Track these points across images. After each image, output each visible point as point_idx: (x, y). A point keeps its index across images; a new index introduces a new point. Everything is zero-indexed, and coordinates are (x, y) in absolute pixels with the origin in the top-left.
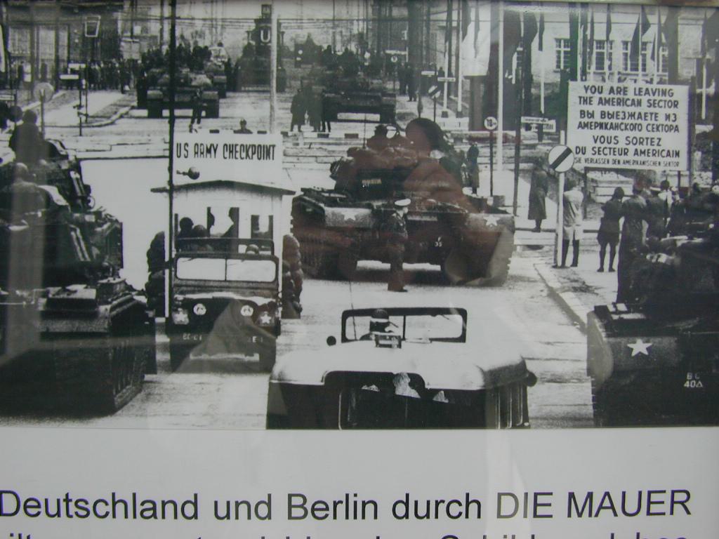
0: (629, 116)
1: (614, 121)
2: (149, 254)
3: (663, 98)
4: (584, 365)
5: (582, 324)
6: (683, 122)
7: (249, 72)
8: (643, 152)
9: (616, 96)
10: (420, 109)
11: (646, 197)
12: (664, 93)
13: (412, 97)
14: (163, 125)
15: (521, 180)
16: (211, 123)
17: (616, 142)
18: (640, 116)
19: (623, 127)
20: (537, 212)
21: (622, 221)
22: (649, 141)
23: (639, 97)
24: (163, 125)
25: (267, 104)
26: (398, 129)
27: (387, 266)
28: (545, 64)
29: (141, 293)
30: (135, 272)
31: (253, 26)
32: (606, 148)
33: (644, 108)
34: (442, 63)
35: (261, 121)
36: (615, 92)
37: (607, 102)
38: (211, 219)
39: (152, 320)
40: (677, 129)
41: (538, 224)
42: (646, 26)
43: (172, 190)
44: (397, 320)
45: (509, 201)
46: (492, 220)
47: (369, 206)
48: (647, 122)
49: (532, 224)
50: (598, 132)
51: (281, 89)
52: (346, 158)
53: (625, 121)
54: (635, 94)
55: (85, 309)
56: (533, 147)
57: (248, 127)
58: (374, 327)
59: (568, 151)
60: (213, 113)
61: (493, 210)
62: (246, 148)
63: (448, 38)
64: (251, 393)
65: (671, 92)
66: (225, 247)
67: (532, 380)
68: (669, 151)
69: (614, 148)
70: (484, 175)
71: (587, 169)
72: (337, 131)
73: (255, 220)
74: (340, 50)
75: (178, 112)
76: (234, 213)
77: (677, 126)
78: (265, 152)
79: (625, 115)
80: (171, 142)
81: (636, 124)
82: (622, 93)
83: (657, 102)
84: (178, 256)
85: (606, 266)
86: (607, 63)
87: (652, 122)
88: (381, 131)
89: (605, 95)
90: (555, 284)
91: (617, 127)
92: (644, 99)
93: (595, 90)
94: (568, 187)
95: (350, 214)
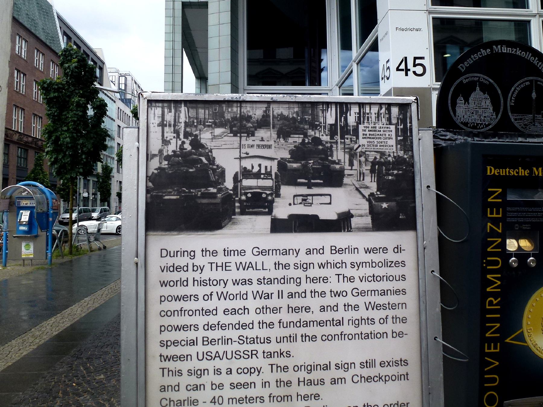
1: (373, 136)
2: (233, 178)
4: (368, 211)
5: (367, 199)
6: (394, 136)
7: (264, 123)
10: (315, 134)
11: (384, 159)
12: (388, 128)
13: (313, 130)
14: (238, 139)
15: (346, 155)
16: (253, 138)
20: (351, 164)
21: (377, 166)
24: (238, 139)
25: (269, 132)
26: (309, 140)
27: (307, 181)
28: (352, 120)
29: (231, 190)
30: (229, 184)
31: (265, 109)
33: (382, 133)
34: (322, 120)
35: (268, 137)
37: (371, 131)
38: (253, 167)
39: (234, 199)
41: (352, 168)
42: (381, 108)
43: (241, 158)
44: (310, 198)
45: (343, 161)
46: (337, 167)
47: (301, 163)
49: (350, 168)
50: (369, 140)
51: (273, 128)
52: (293, 148)
55: (213, 196)
56: (349, 144)
57: (264, 139)
58: (303, 200)
59: (360, 146)
60: (253, 135)
61: (338, 164)
62: (263, 146)
63: (323, 113)
64: (265, 221)
66: (257, 176)
67: (352, 216)
70: (335, 153)
71: (366, 151)
72: (291, 140)
73: (266, 167)
74: (291, 116)
75: (242, 135)
76: (260, 165)
78: (270, 147)
80: (240, 144)
84: (243, 179)
85: (373, 180)
86: (370, 119)
88: (303, 140)
89: (370, 129)
90: (358, 186)
91: (374, 138)
93: (367, 127)
94: (360, 156)
95: (295, 165)
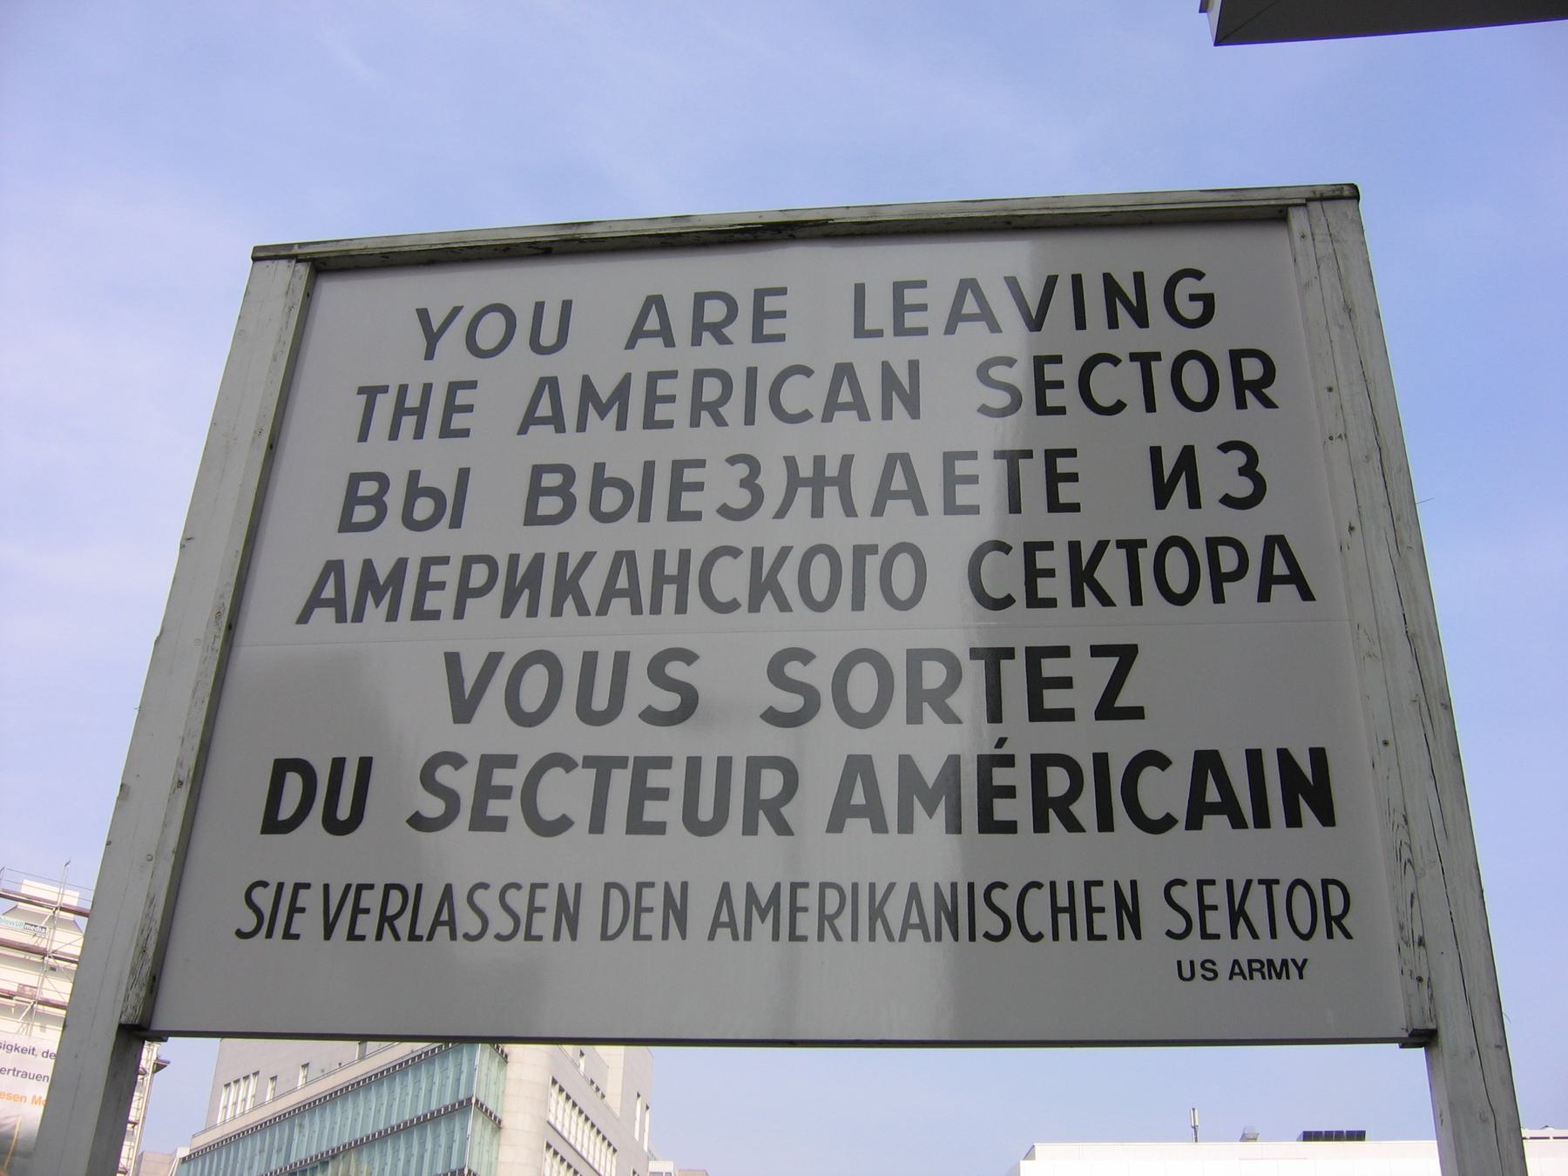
0: (794, 481)
1: (648, 537)
3: (1128, 337)
9: (686, 358)
17: (669, 701)
19: (731, 579)
22: (1014, 674)
23: (899, 351)
32: (561, 761)
40: (1281, 569)
50: (486, 631)
54: (860, 331)
65: (1186, 287)
68: (1207, 763)
69: (644, 765)
77: (1275, 543)
79: (749, 483)
82: (740, 329)
83: (1067, 372)
91: (679, 581)
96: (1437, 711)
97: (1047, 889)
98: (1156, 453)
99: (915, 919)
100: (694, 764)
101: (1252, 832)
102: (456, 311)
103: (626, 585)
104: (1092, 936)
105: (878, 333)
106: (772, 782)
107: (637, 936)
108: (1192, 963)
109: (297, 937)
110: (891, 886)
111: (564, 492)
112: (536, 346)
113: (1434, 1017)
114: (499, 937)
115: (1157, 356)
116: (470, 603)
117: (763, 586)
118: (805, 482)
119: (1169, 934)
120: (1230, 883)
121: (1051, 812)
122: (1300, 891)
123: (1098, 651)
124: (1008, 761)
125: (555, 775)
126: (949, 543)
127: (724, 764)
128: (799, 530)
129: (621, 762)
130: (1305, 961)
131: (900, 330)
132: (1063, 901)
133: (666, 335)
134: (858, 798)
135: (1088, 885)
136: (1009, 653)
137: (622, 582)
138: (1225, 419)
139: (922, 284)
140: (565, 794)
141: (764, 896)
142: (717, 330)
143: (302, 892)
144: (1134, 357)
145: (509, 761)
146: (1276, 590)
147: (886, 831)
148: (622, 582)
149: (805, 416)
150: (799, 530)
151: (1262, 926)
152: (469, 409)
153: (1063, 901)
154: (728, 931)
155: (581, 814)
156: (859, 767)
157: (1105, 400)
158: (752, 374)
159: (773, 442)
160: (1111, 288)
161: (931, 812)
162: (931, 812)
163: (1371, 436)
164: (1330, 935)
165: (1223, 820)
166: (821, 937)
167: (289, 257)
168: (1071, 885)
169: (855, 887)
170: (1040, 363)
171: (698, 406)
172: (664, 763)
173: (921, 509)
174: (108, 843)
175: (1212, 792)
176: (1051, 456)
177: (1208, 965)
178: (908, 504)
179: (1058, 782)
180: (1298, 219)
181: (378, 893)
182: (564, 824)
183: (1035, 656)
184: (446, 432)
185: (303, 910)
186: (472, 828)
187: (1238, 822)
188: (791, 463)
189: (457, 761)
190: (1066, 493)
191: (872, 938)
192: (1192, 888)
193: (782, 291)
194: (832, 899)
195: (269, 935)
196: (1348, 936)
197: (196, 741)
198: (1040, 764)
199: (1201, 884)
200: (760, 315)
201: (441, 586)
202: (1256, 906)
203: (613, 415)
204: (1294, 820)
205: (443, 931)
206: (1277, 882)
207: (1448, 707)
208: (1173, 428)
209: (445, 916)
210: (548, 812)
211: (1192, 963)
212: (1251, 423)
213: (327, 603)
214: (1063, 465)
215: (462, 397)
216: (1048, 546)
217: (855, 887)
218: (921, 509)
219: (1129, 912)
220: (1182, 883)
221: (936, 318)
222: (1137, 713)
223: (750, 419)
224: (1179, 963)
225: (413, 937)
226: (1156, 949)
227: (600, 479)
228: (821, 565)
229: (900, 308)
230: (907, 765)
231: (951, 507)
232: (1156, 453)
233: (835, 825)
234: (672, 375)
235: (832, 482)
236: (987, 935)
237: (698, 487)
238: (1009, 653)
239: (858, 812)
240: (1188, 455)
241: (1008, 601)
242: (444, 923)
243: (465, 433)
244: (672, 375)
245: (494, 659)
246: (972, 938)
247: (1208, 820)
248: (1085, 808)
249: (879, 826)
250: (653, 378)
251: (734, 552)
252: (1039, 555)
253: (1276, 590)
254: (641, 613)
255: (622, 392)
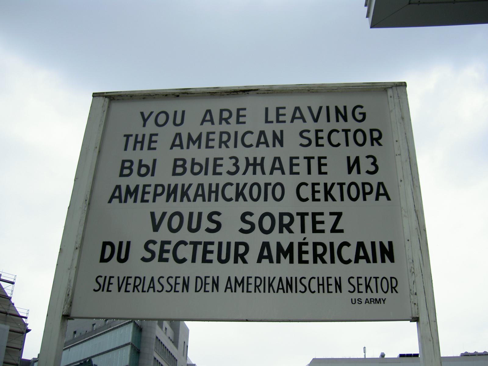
3: (342, 125)
8: (286, 252)
9: (218, 128)
17: (213, 226)
18: (277, 165)
19: (230, 192)
22: (308, 220)
36: (216, 119)
40: (382, 192)
48: (297, 180)
50: (162, 206)
53: (233, 179)
54: (267, 121)
65: (358, 110)
68: (360, 245)
69: (206, 244)
77: (380, 184)
79: (235, 165)
81: (267, 185)
82: (233, 120)
83: (324, 134)
87: (310, 180)
91: (216, 192)
92: (292, 131)
96: (422, 231)
97: (316, 279)
98: (348, 158)
99: (281, 287)
100: (220, 244)
101: (372, 264)
102: (152, 113)
103: (200, 193)
104: (328, 292)
105: (272, 122)
106: (242, 249)
107: (205, 291)
108: (355, 299)
109: (110, 291)
110: (274, 278)
111: (183, 166)
112: (175, 124)
113: (418, 314)
114: (167, 291)
115: (349, 130)
116: (157, 198)
117: (239, 194)
118: (251, 165)
119: (349, 291)
120: (366, 278)
121: (318, 258)
122: (384, 280)
123: (331, 214)
124: (306, 244)
125: (181, 246)
126: (290, 182)
127: (229, 244)
128: (249, 178)
129: (200, 243)
130: (385, 299)
131: (278, 121)
132: (321, 282)
133: (212, 121)
134: (266, 253)
135: (328, 278)
136: (307, 214)
137: (200, 192)
138: (368, 149)
139: (284, 108)
140: (185, 252)
141: (240, 281)
142: (226, 120)
143: (112, 279)
144: (343, 130)
145: (169, 243)
146: (380, 197)
147: (273, 263)
148: (200, 192)
149: (251, 146)
150: (249, 178)
151: (374, 289)
152: (156, 142)
153: (321, 282)
154: (230, 290)
155: (189, 257)
156: (266, 245)
157: (335, 143)
158: (236, 133)
159: (242, 153)
160: (337, 110)
161: (285, 258)
162: (285, 258)
163: (407, 155)
164: (392, 292)
165: (364, 261)
166: (255, 292)
167: (103, 96)
168: (323, 278)
169: (265, 278)
170: (317, 131)
171: (221, 142)
172: (212, 243)
173: (283, 173)
174: (57, 265)
175: (362, 253)
176: (320, 158)
177: (359, 300)
178: (279, 171)
179: (320, 250)
180: (390, 92)
181: (133, 279)
182: (184, 260)
183: (314, 215)
184: (149, 148)
185: (112, 284)
186: (159, 261)
187: (368, 261)
188: (247, 159)
189: (154, 242)
190: (324, 169)
191: (269, 292)
192: (356, 279)
193: (245, 109)
194: (258, 280)
195: (103, 290)
196: (397, 292)
197: (81, 236)
198: (315, 245)
199: (358, 278)
200: (238, 116)
201: (149, 193)
202: (373, 284)
203: (197, 144)
204: (383, 261)
205: (151, 290)
206: (378, 278)
207: (425, 230)
208: (353, 151)
209: (152, 286)
210: (180, 257)
211: (355, 299)
212: (375, 150)
213: (116, 197)
214: (323, 161)
215: (154, 138)
216: (318, 184)
217: (265, 278)
218: (283, 173)
219: (339, 286)
220: (353, 278)
221: (288, 118)
222: (342, 231)
223: (236, 146)
224: (352, 299)
225: (143, 291)
226: (345, 295)
227: (193, 163)
228: (255, 188)
229: (278, 115)
230: (279, 245)
231: (292, 173)
232: (348, 158)
233: (259, 261)
234: (214, 133)
235: (258, 165)
236: (300, 291)
237: (221, 165)
238: (307, 214)
239: (265, 257)
240: (357, 160)
241: (307, 199)
242: (152, 287)
243: (155, 149)
244: (214, 133)
245: (164, 214)
246: (296, 292)
247: (360, 261)
248: (327, 257)
249: (271, 261)
250: (208, 134)
251: (231, 184)
252: (316, 186)
253: (380, 197)
254: (205, 201)
255: (199, 137)
